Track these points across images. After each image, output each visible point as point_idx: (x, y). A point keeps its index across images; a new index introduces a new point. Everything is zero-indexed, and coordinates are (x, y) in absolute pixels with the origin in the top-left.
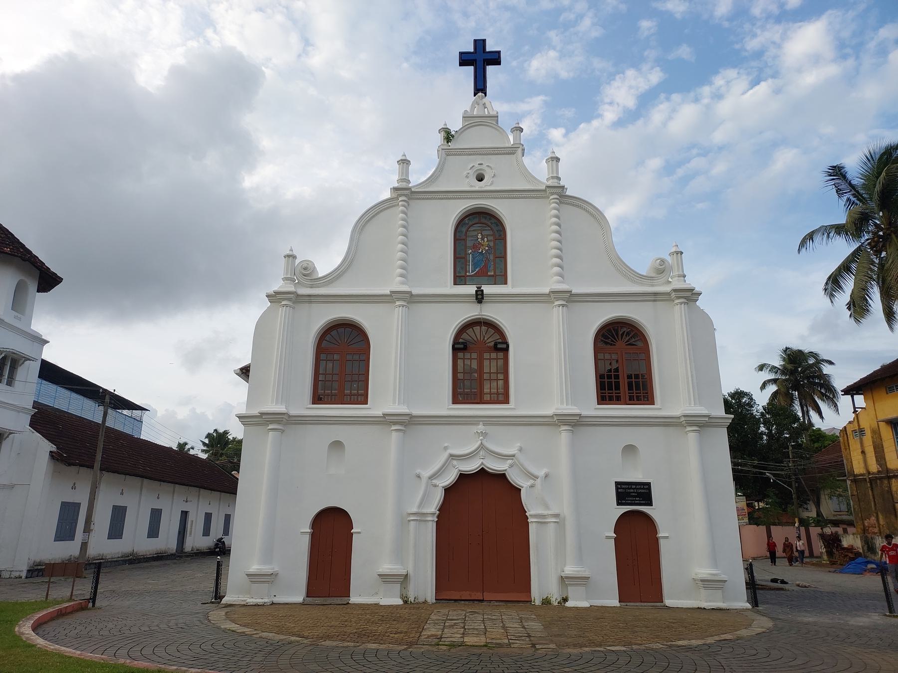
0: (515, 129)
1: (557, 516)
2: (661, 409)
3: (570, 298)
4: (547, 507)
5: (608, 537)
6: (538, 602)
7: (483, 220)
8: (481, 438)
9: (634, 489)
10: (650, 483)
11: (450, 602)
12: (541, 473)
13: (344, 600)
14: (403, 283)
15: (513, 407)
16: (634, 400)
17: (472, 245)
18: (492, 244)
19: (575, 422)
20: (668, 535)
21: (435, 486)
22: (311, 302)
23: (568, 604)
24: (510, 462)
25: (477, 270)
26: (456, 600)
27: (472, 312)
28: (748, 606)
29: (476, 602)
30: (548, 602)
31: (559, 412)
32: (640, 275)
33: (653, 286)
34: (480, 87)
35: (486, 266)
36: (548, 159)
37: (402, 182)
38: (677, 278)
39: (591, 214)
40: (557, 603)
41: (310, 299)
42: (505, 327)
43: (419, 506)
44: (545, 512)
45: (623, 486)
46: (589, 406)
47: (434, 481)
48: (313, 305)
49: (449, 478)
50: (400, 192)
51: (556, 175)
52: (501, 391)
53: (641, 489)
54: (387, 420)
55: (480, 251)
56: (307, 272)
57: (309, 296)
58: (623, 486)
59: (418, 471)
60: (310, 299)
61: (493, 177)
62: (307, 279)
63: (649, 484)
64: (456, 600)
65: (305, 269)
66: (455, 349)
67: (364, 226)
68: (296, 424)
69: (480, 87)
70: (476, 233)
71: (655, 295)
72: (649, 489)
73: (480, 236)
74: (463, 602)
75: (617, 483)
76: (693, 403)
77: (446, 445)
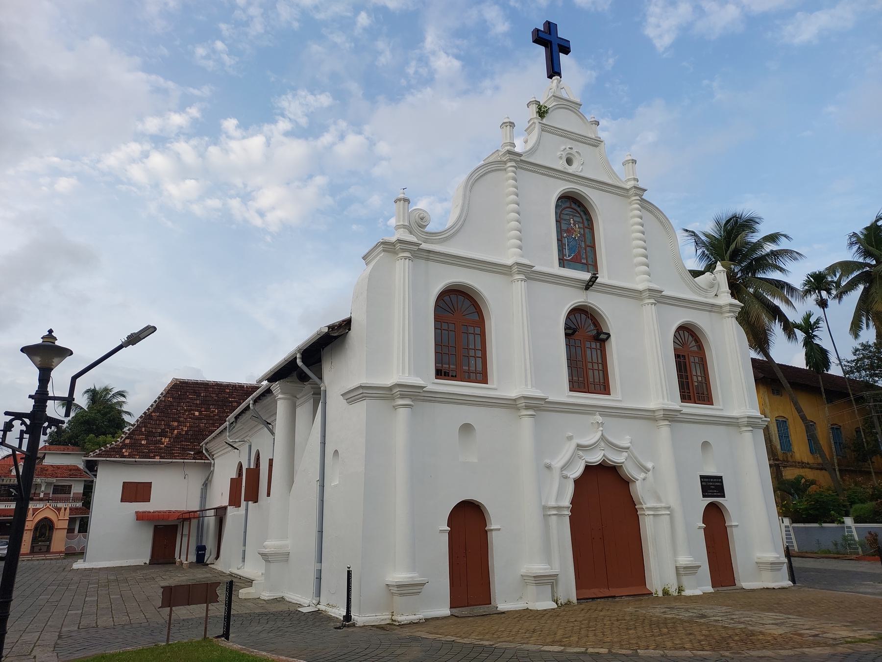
0: (594, 122)
1: (668, 508)
2: (722, 410)
3: (659, 297)
4: (659, 499)
5: (700, 528)
6: (660, 594)
7: (573, 206)
8: (601, 428)
9: (712, 482)
10: (722, 477)
11: (588, 600)
12: (649, 465)
13: (482, 609)
14: (522, 256)
15: (620, 398)
16: (704, 401)
17: (566, 229)
18: (582, 232)
19: (671, 417)
20: (737, 524)
21: (566, 477)
22: (428, 259)
23: (683, 593)
24: (625, 454)
25: (573, 255)
26: (593, 599)
27: (578, 298)
28: (791, 583)
29: (610, 599)
30: (666, 592)
31: (666, 407)
32: (699, 286)
33: (706, 297)
34: (554, 71)
35: (579, 252)
36: (629, 160)
37: (510, 146)
38: (726, 294)
39: (661, 222)
40: (677, 593)
41: (429, 255)
42: (608, 320)
43: (557, 500)
44: (658, 505)
45: (705, 480)
46: (674, 402)
47: (565, 472)
48: (431, 263)
49: (577, 471)
50: (512, 157)
51: (633, 177)
52: (602, 381)
53: (716, 482)
54: (511, 405)
55: (574, 236)
56: (419, 223)
57: (429, 251)
58: (705, 480)
59: (548, 461)
60: (429, 255)
61: (582, 165)
62: (419, 229)
63: (721, 478)
64: (593, 599)
65: (422, 219)
66: (567, 335)
67: (473, 184)
68: (424, 400)
69: (554, 71)
70: (567, 217)
71: (712, 307)
72: (722, 482)
73: (572, 221)
74: (599, 600)
75: (702, 477)
76: (748, 406)
77: (571, 434)
